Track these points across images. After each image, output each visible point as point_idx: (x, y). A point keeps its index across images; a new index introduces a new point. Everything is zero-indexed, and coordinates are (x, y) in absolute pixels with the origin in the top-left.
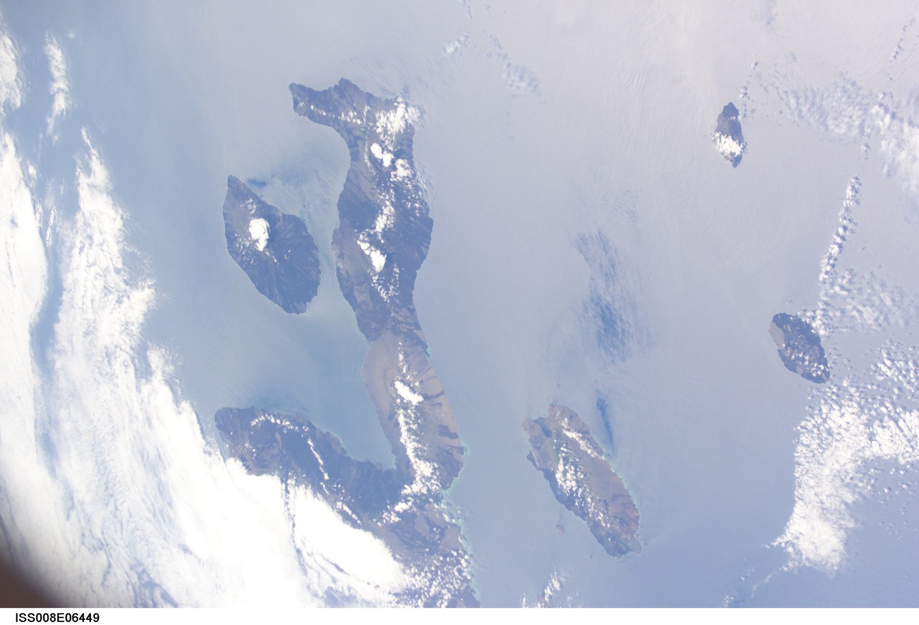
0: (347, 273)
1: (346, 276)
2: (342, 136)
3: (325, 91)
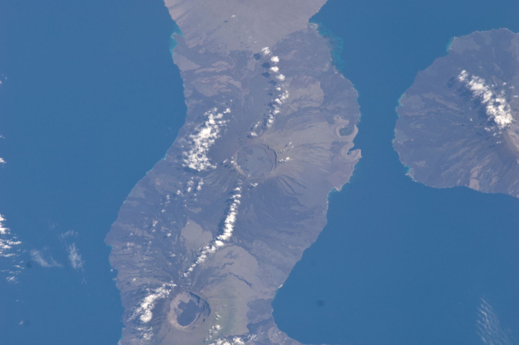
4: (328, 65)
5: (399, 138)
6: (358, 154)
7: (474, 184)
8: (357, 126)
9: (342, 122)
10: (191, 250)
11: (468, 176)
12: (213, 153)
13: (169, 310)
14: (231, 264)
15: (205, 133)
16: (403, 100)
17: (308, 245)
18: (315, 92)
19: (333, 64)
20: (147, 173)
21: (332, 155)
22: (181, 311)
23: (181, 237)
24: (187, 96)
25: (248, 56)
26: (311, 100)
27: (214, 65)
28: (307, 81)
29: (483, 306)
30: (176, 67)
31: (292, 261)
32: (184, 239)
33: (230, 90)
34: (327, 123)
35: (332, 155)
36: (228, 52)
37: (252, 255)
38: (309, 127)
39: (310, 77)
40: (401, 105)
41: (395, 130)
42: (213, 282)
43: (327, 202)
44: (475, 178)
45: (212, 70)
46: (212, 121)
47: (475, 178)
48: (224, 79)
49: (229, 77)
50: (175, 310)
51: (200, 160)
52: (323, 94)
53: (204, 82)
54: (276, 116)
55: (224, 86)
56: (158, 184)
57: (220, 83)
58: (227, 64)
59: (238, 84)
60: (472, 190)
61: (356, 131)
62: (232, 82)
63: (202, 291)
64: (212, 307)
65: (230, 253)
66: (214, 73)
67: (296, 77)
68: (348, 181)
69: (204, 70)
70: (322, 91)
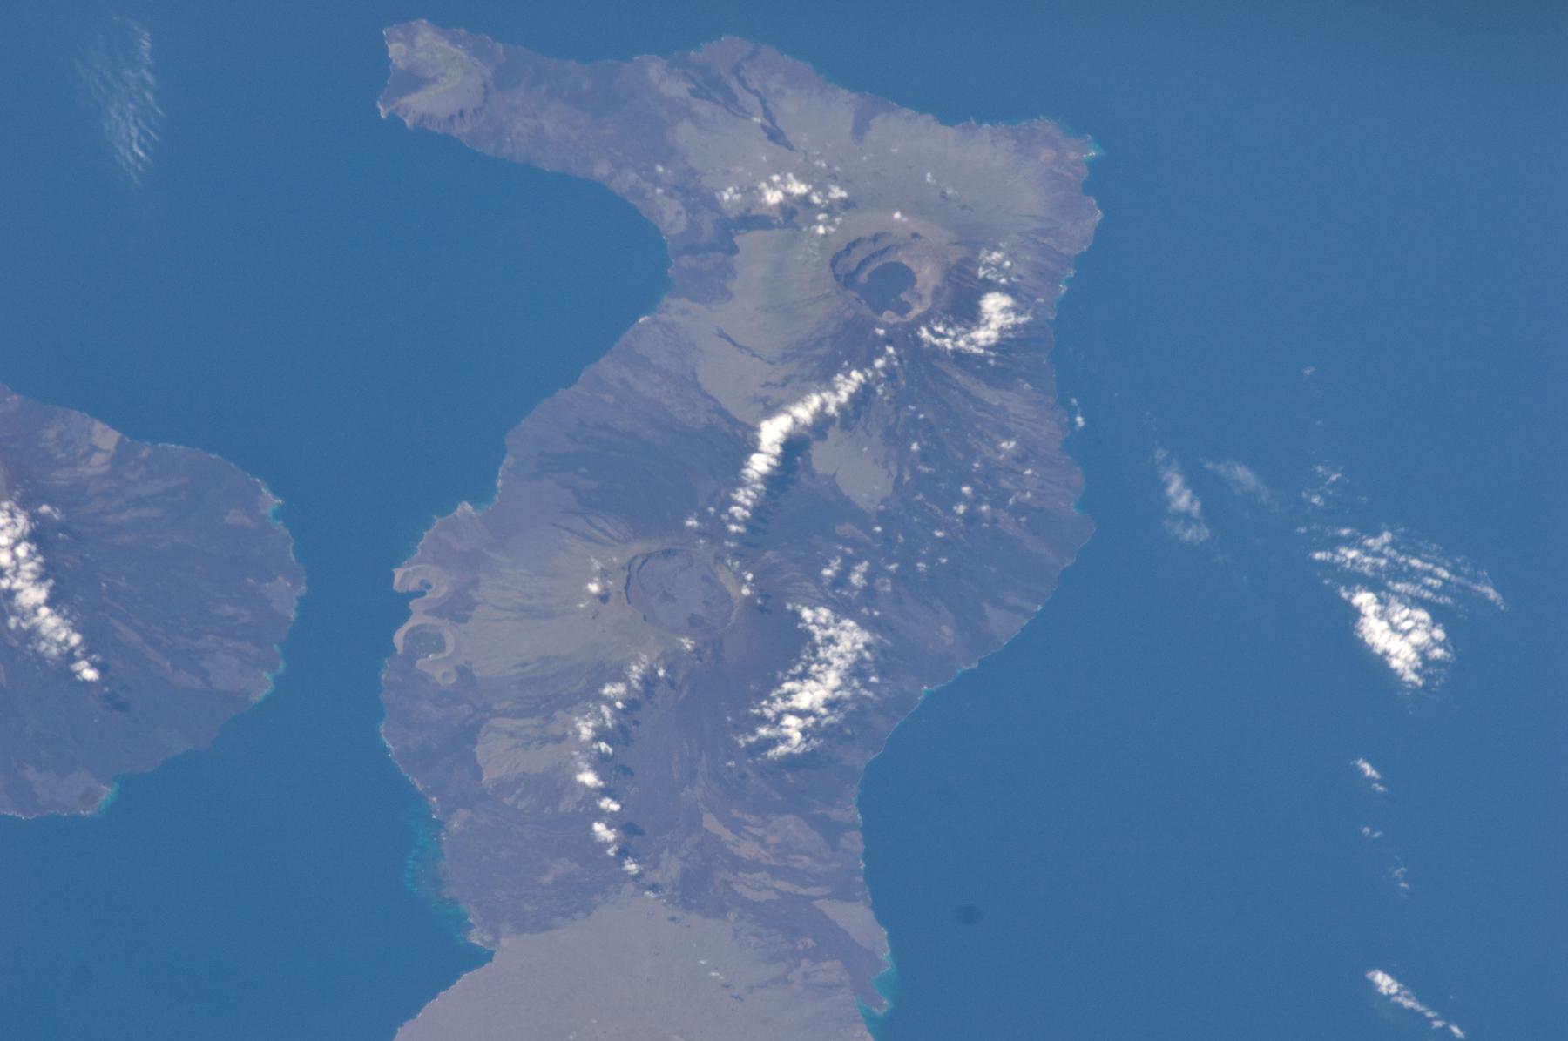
4: (455, 825)
5: (285, 595)
6: (403, 578)
7: (107, 438)
8: (394, 649)
9: (437, 668)
11: (120, 456)
12: (793, 651)
13: (937, 292)
14: (767, 384)
15: (810, 695)
16: (262, 687)
17: (562, 394)
18: (500, 755)
19: (440, 824)
20: (975, 665)
21: (472, 592)
22: (904, 297)
23: (895, 474)
24: (856, 835)
25: (678, 893)
26: (512, 735)
27: (775, 897)
28: (519, 791)
29: (140, 167)
30: (884, 912)
31: (608, 367)
32: (885, 466)
33: (735, 813)
34: (477, 674)
35: (472, 592)
36: (732, 916)
37: (710, 397)
38: (525, 664)
39: (506, 800)
40: (267, 676)
41: (293, 615)
42: (820, 342)
43: (499, 483)
44: (101, 451)
45: (782, 885)
46: (791, 721)
47: (101, 451)
49: (736, 851)
50: (920, 298)
51: (831, 632)
52: (478, 749)
53: (806, 859)
54: (618, 676)
56: (945, 628)
57: (761, 840)
58: (738, 888)
59: (711, 823)
60: (114, 425)
61: (399, 638)
62: (727, 835)
63: (849, 314)
64: (826, 269)
66: (776, 872)
67: (548, 810)
68: (438, 521)
69: (802, 891)
70: (480, 760)
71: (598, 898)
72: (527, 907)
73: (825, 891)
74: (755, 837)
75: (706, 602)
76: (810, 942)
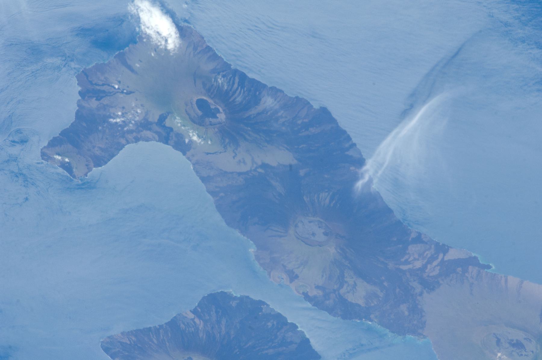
0: (318, 287)
1: (321, 293)
2: (147, 140)
3: (77, 113)
10: (266, 147)
14: (234, 157)
25: (427, 289)
26: (348, 292)
27: (439, 267)
33: (403, 260)
36: (441, 282)
37: (232, 173)
38: (323, 276)
39: (372, 305)
45: (435, 263)
48: (418, 264)
53: (427, 252)
55: (409, 260)
58: (431, 275)
59: (404, 268)
62: (410, 266)
65: (244, 163)
66: (429, 262)
71: (419, 307)
72: (415, 323)
73: (441, 256)
74: (413, 260)
75: (319, 227)
76: (459, 269)
